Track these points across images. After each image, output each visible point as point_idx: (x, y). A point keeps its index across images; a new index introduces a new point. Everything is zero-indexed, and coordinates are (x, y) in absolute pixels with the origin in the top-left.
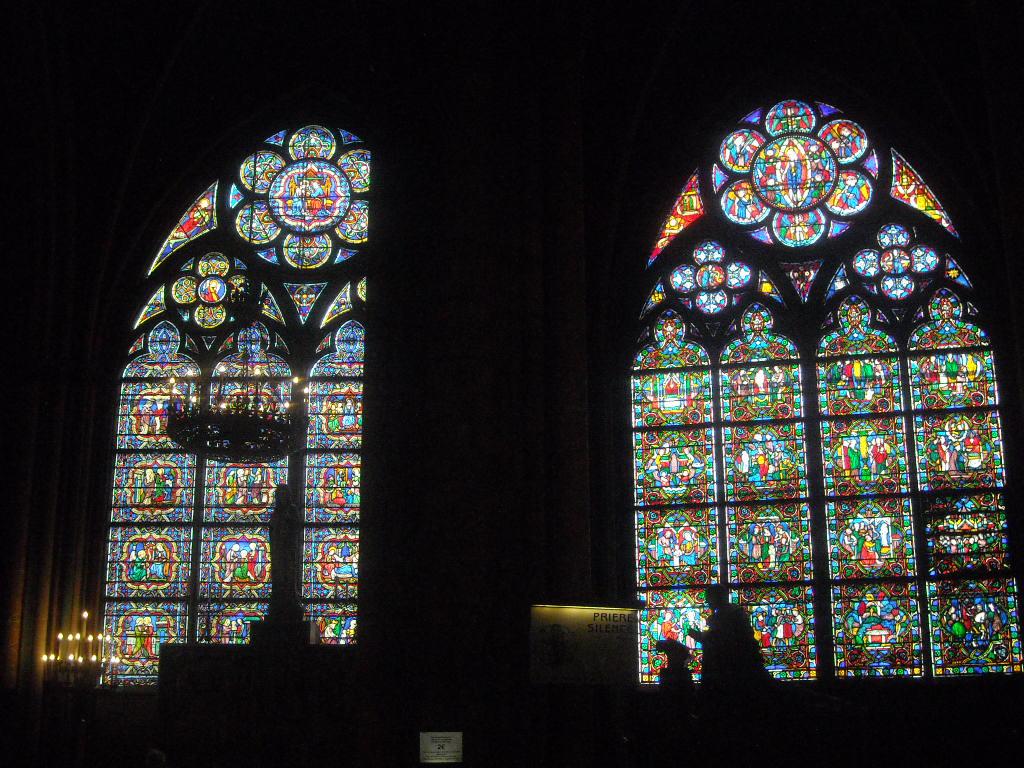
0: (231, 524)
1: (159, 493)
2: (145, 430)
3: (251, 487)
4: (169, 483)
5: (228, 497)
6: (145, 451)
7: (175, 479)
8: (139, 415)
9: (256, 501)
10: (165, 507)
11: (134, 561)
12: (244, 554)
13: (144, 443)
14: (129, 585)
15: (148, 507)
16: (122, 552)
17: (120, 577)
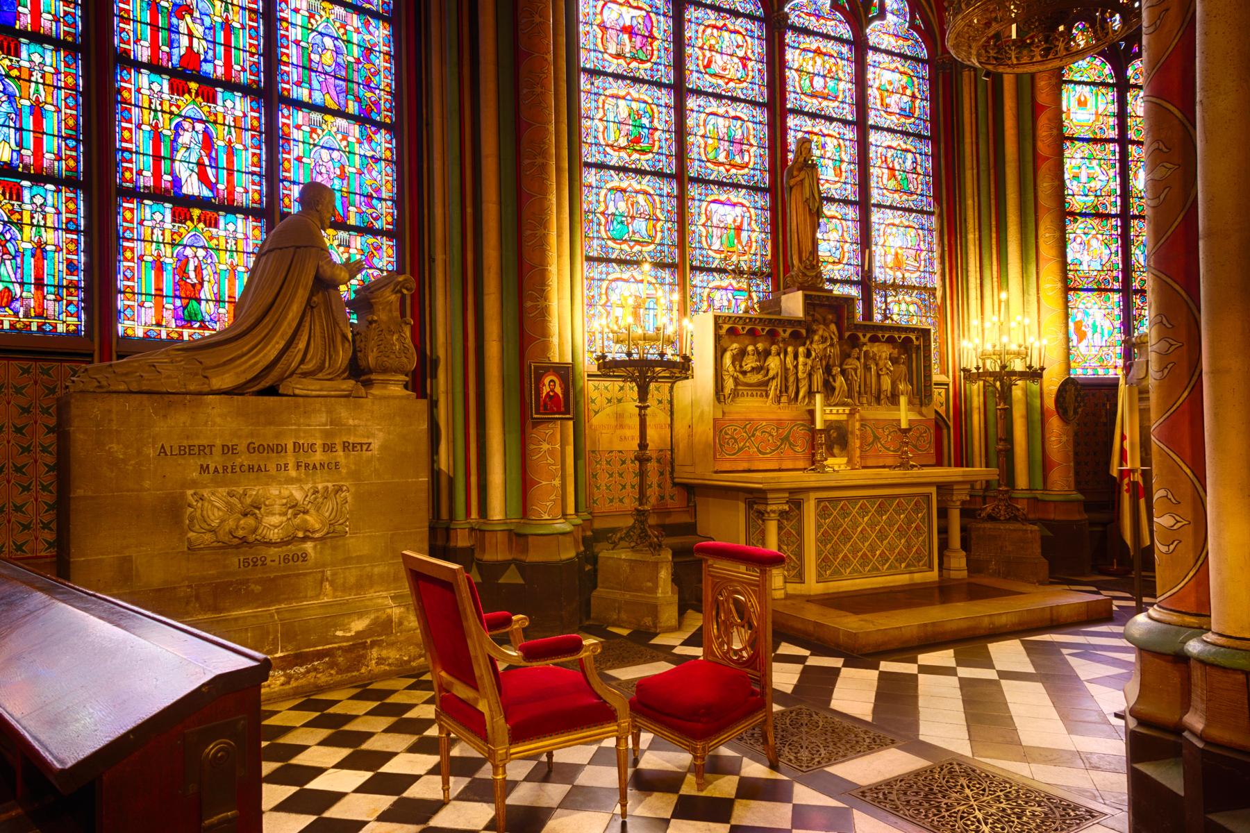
0: (714, 182)
1: (635, 132)
2: (613, 49)
3: (732, 142)
4: (645, 121)
5: (709, 149)
6: (617, 76)
7: (652, 117)
8: (603, 27)
9: (738, 160)
10: (643, 152)
11: (613, 214)
12: (730, 220)
13: (613, 66)
14: (610, 243)
15: (624, 148)
16: (598, 201)
17: (598, 232)
